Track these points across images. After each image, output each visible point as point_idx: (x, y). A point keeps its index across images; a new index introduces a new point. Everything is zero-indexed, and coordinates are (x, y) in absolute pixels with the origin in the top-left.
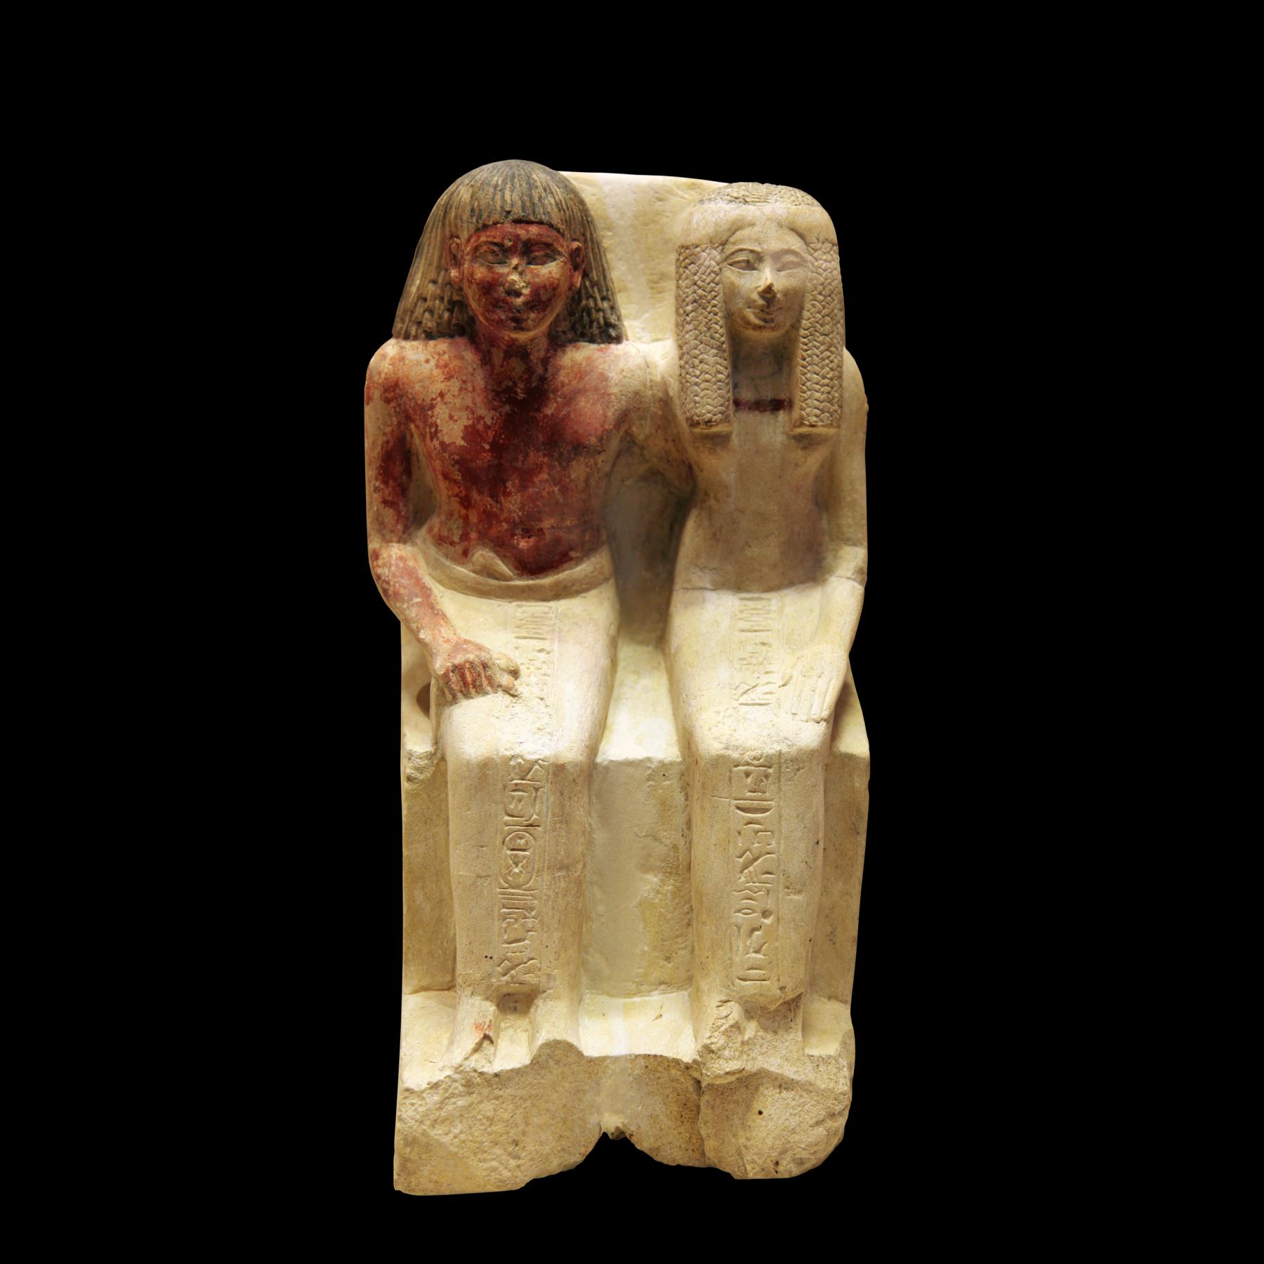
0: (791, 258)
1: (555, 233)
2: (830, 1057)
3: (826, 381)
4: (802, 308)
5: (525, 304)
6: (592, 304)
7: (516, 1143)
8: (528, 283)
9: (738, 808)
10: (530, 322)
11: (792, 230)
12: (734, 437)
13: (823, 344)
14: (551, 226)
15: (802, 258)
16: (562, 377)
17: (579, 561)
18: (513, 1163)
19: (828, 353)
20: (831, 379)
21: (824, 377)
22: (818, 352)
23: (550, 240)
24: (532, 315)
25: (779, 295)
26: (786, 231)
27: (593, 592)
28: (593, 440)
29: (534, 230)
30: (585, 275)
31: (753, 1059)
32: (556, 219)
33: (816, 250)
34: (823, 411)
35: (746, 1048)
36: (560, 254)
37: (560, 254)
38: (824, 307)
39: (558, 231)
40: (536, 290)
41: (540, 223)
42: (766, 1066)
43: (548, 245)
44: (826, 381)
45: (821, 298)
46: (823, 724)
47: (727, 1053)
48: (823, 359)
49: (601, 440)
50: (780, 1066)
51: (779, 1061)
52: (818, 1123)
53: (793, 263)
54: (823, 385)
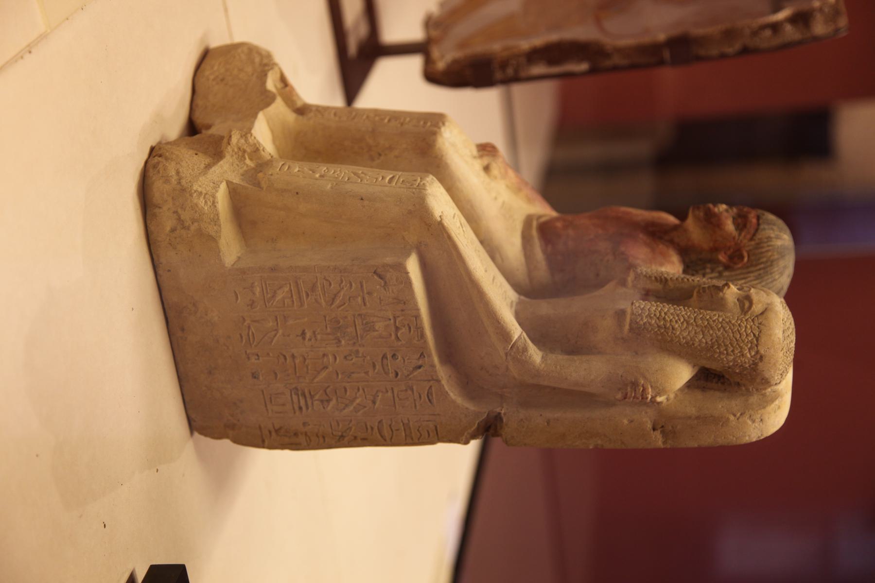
0: (747, 304)
1: (752, 231)
2: (217, 191)
3: (663, 314)
4: (712, 310)
5: (709, 209)
6: (708, 270)
7: (222, 80)
8: (721, 213)
9: (393, 177)
10: (697, 212)
11: (766, 309)
12: (624, 289)
13: (689, 317)
14: (757, 230)
15: (747, 312)
16: (661, 246)
17: (544, 252)
18: (212, 77)
19: (682, 320)
20: (664, 319)
21: (665, 314)
22: (683, 313)
23: (748, 226)
24: (702, 214)
25: (721, 294)
26: (765, 306)
27: (523, 259)
28: (623, 249)
29: (754, 221)
30: (727, 268)
31: (232, 156)
32: (760, 235)
33: (753, 320)
34: (642, 309)
35: (240, 154)
36: (740, 234)
37: (740, 234)
38: (714, 321)
39: (754, 235)
40: (715, 215)
41: (758, 224)
42: (225, 160)
43: (745, 226)
44: (663, 314)
45: (721, 320)
46: (439, 219)
47: (243, 141)
48: (678, 315)
49: (623, 253)
50: (222, 167)
51: (225, 168)
52: (178, 173)
53: (744, 305)
54: (660, 312)
